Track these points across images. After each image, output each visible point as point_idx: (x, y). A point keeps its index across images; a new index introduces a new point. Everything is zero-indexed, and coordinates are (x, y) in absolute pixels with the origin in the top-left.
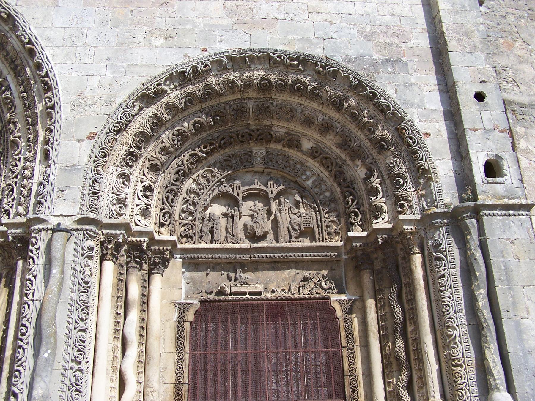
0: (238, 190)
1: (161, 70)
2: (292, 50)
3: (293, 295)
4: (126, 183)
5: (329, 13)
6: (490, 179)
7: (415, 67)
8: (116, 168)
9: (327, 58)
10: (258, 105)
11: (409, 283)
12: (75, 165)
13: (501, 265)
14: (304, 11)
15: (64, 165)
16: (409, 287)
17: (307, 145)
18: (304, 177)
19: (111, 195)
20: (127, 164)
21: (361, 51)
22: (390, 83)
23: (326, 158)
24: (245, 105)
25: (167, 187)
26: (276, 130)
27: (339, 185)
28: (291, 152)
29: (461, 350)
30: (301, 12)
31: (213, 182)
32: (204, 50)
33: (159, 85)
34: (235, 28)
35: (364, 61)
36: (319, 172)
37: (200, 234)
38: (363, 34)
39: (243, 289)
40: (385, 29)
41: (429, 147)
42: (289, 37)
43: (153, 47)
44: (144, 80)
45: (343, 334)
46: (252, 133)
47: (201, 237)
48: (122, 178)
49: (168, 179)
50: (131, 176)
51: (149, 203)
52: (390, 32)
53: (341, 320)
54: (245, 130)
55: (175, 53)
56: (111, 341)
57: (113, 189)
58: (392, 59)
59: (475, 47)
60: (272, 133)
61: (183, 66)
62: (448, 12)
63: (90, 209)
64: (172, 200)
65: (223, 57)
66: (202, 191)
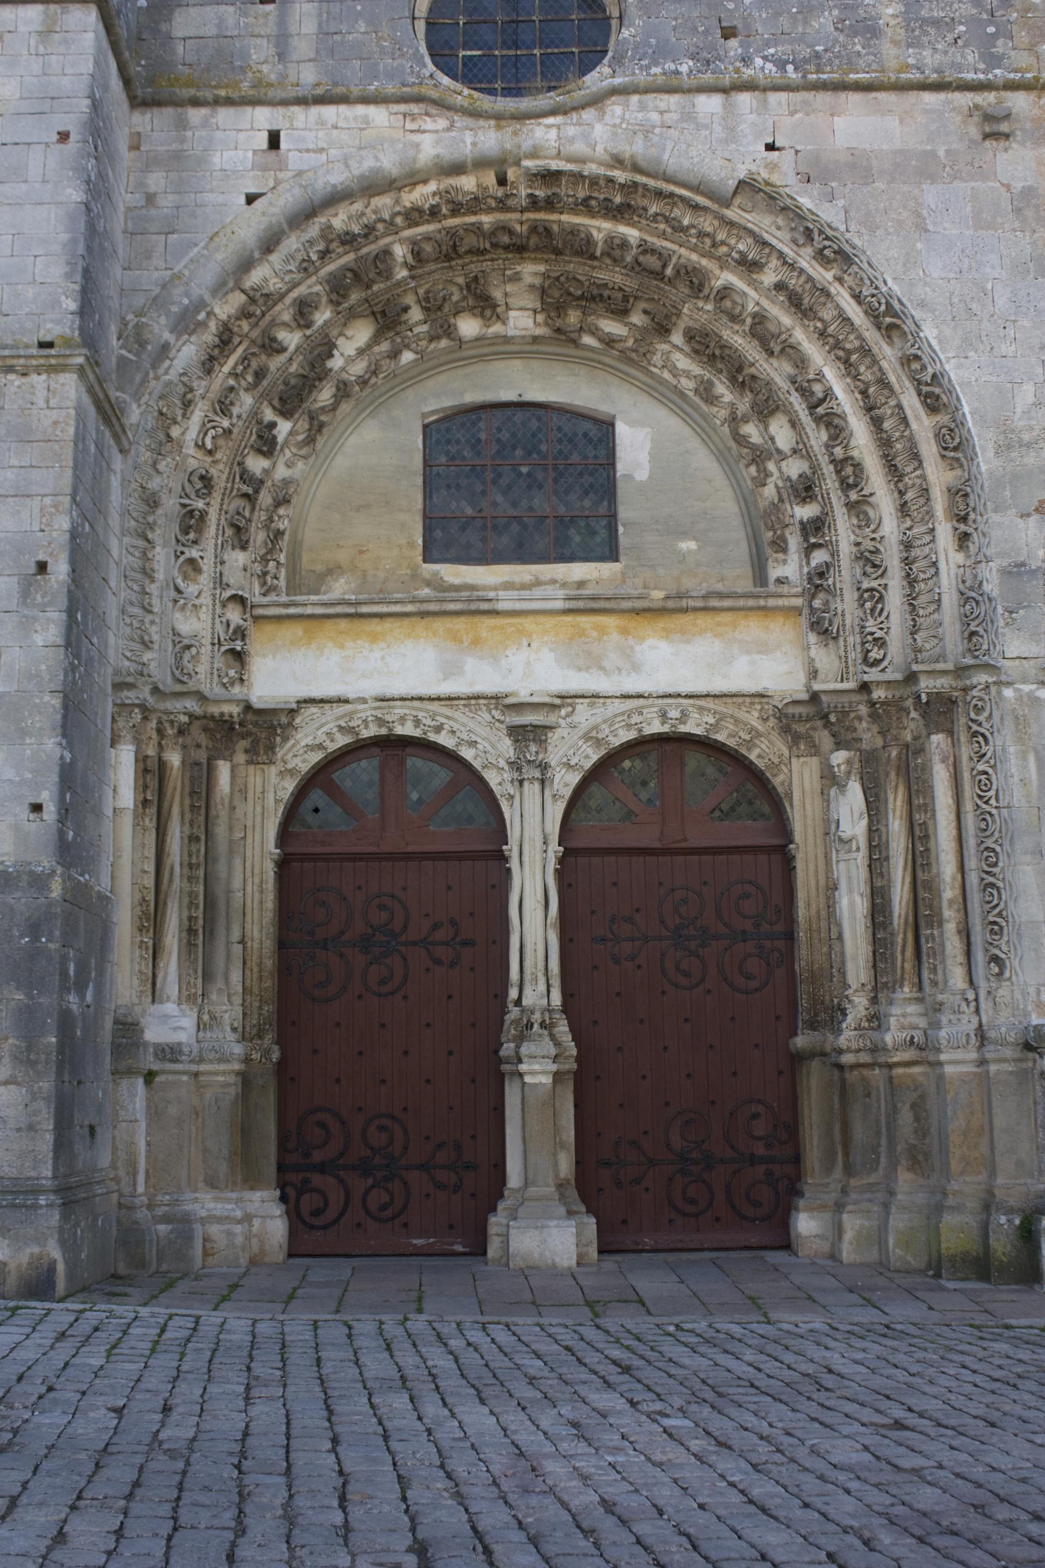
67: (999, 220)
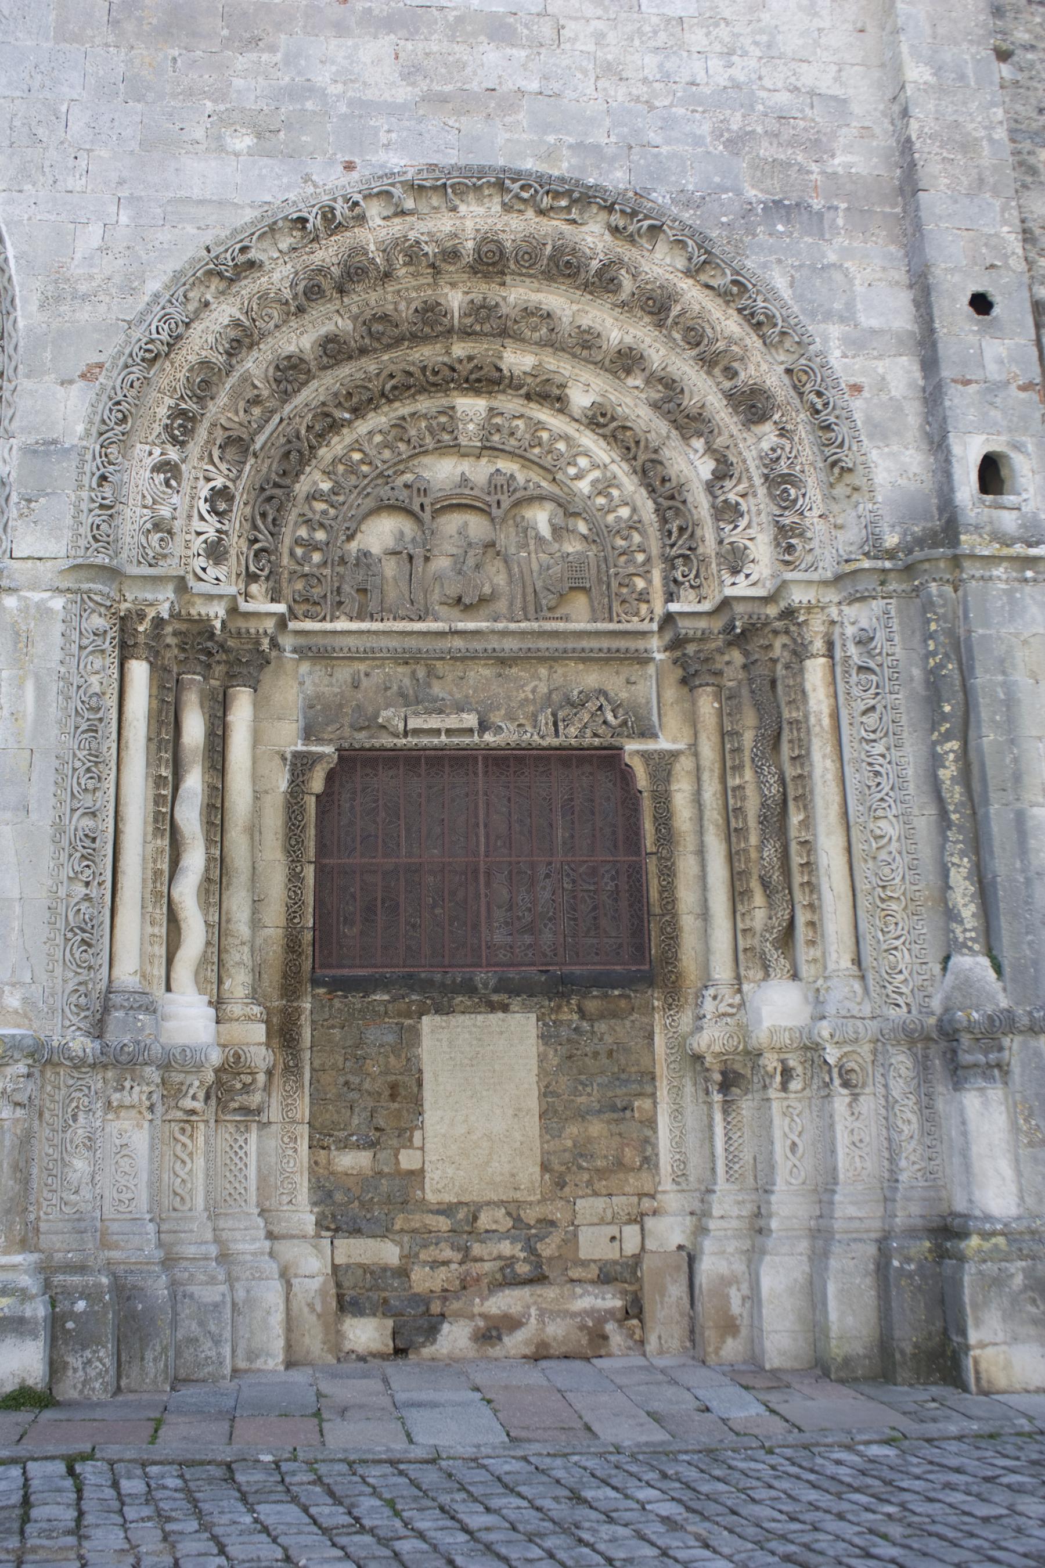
0: (422, 499)
1: (249, 215)
2: (556, 173)
3: (542, 737)
4: (173, 483)
5: (645, 81)
6: (989, 498)
7: (840, 222)
8: (147, 448)
9: (636, 194)
10: (472, 301)
11: (798, 722)
12: (54, 442)
13: (999, 690)
14: (585, 73)
15: (31, 440)
16: (798, 730)
17: (580, 399)
18: (572, 471)
19: (138, 510)
20: (174, 438)
21: (717, 179)
22: (779, 261)
23: (625, 428)
24: (442, 301)
25: (262, 489)
26: (512, 360)
27: (652, 490)
28: (543, 414)
29: (900, 870)
30: (579, 76)
31: (365, 477)
32: (349, 167)
33: (244, 250)
34: (421, 112)
35: (723, 205)
36: (608, 460)
37: (338, 599)
38: (722, 136)
39: (434, 722)
40: (773, 125)
41: (858, 416)
42: (551, 139)
43: (227, 153)
44: (208, 238)
45: (648, 826)
46: (457, 366)
47: (340, 603)
48: (165, 472)
49: (265, 470)
50: (183, 467)
51: (224, 528)
52: (787, 133)
53: (645, 794)
54: (440, 359)
55: (280, 172)
56: (149, 837)
57: (144, 497)
58: (787, 202)
59: (981, 181)
60: (504, 367)
61: (301, 206)
62: (925, 91)
63: (95, 545)
64: (274, 520)
65: (393, 185)
66: (341, 499)
67: (89, 32)
